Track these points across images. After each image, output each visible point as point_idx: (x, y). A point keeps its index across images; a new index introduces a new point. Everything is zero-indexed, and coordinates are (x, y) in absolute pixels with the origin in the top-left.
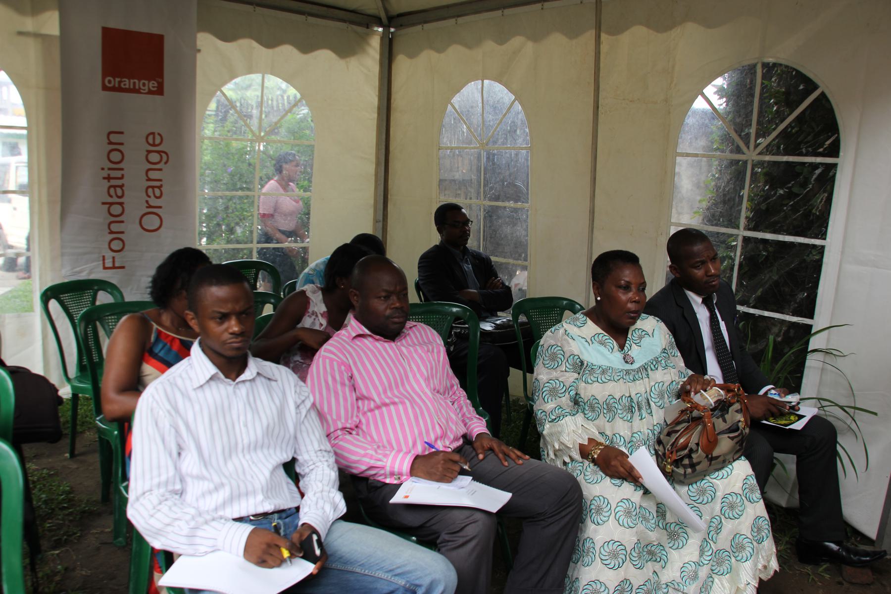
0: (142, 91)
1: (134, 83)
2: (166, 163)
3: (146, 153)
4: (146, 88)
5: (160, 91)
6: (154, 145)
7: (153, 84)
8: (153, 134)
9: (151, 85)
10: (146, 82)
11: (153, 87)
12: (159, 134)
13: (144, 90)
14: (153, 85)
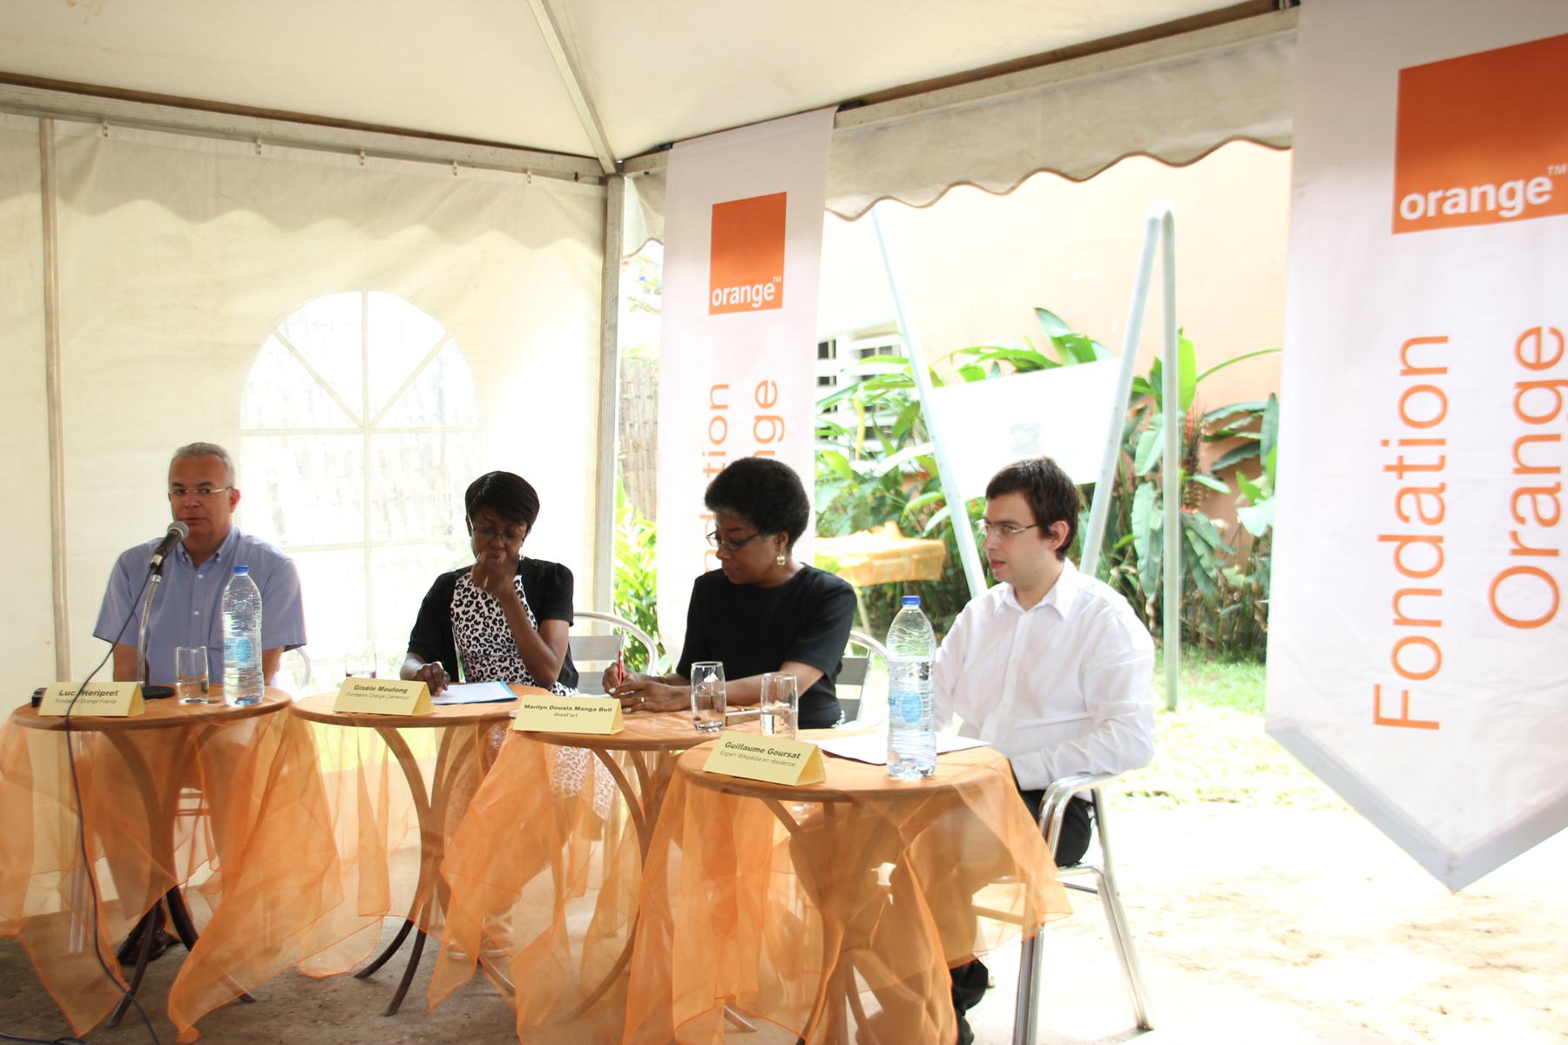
0: (755, 305)
1: (746, 291)
2: (780, 439)
3: (754, 422)
4: (760, 298)
5: (776, 302)
6: (766, 406)
7: (769, 288)
8: (765, 383)
9: (766, 291)
10: (760, 287)
11: (769, 294)
12: (774, 384)
13: (757, 302)
14: (766, 291)
